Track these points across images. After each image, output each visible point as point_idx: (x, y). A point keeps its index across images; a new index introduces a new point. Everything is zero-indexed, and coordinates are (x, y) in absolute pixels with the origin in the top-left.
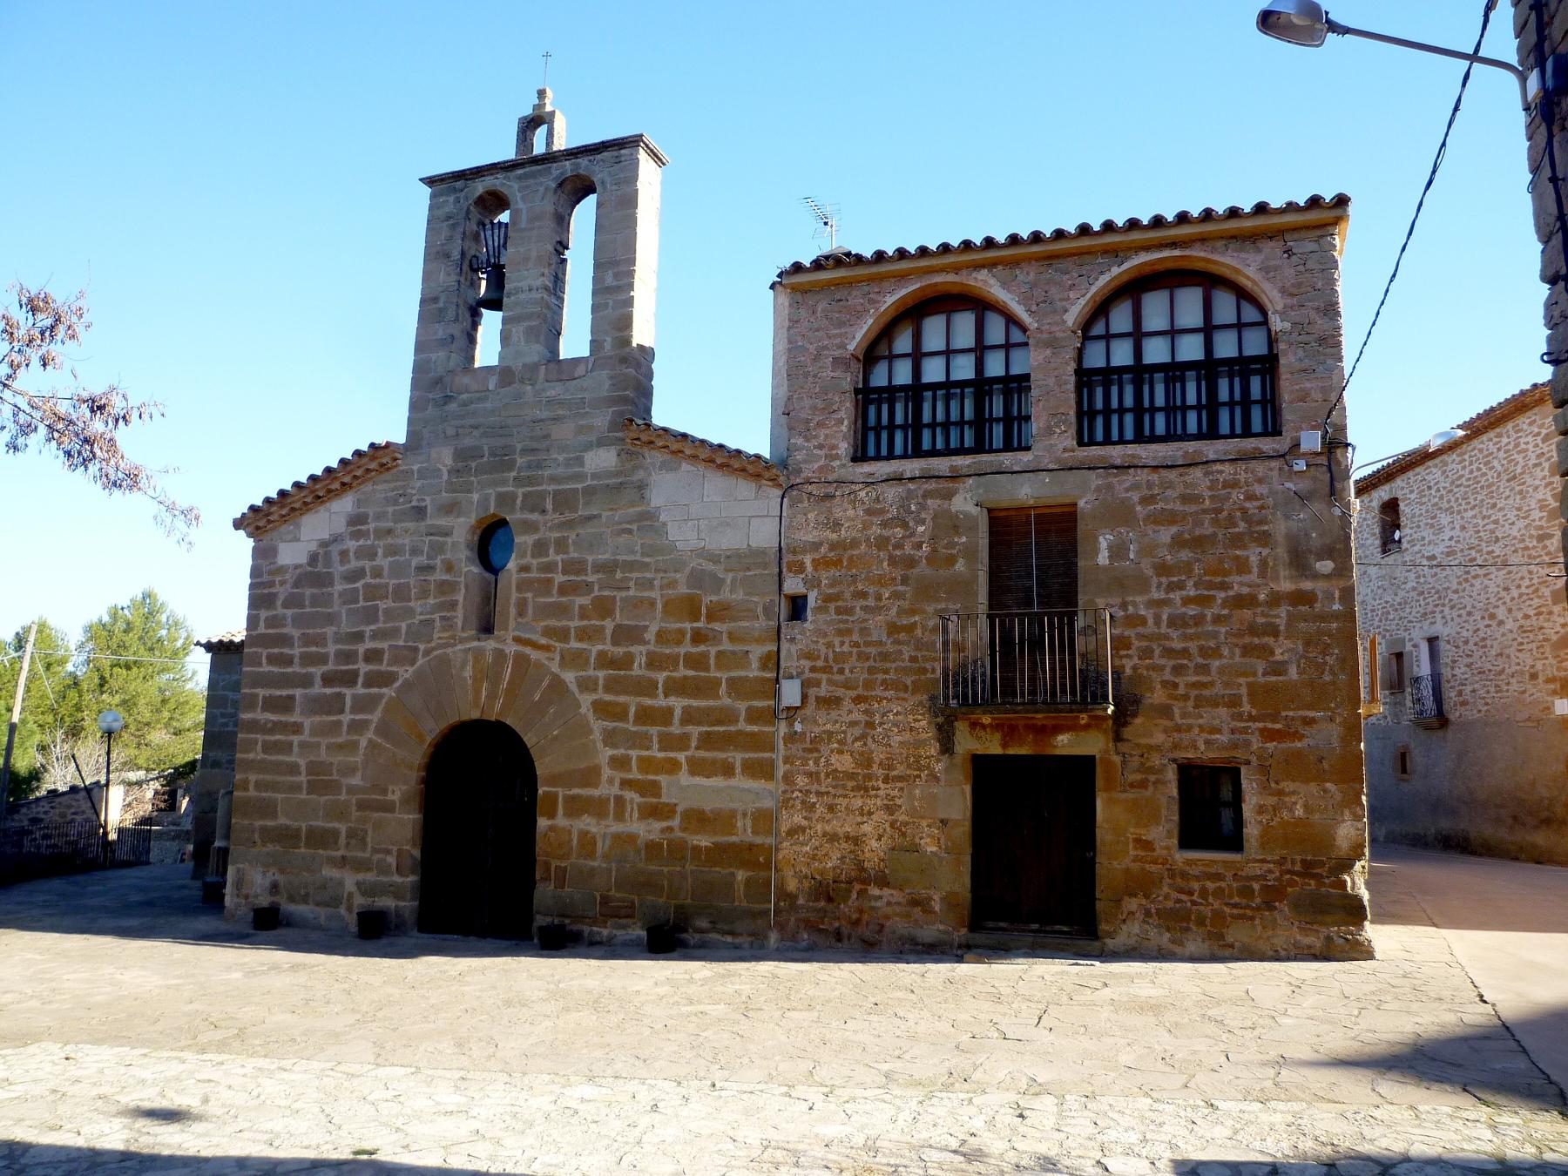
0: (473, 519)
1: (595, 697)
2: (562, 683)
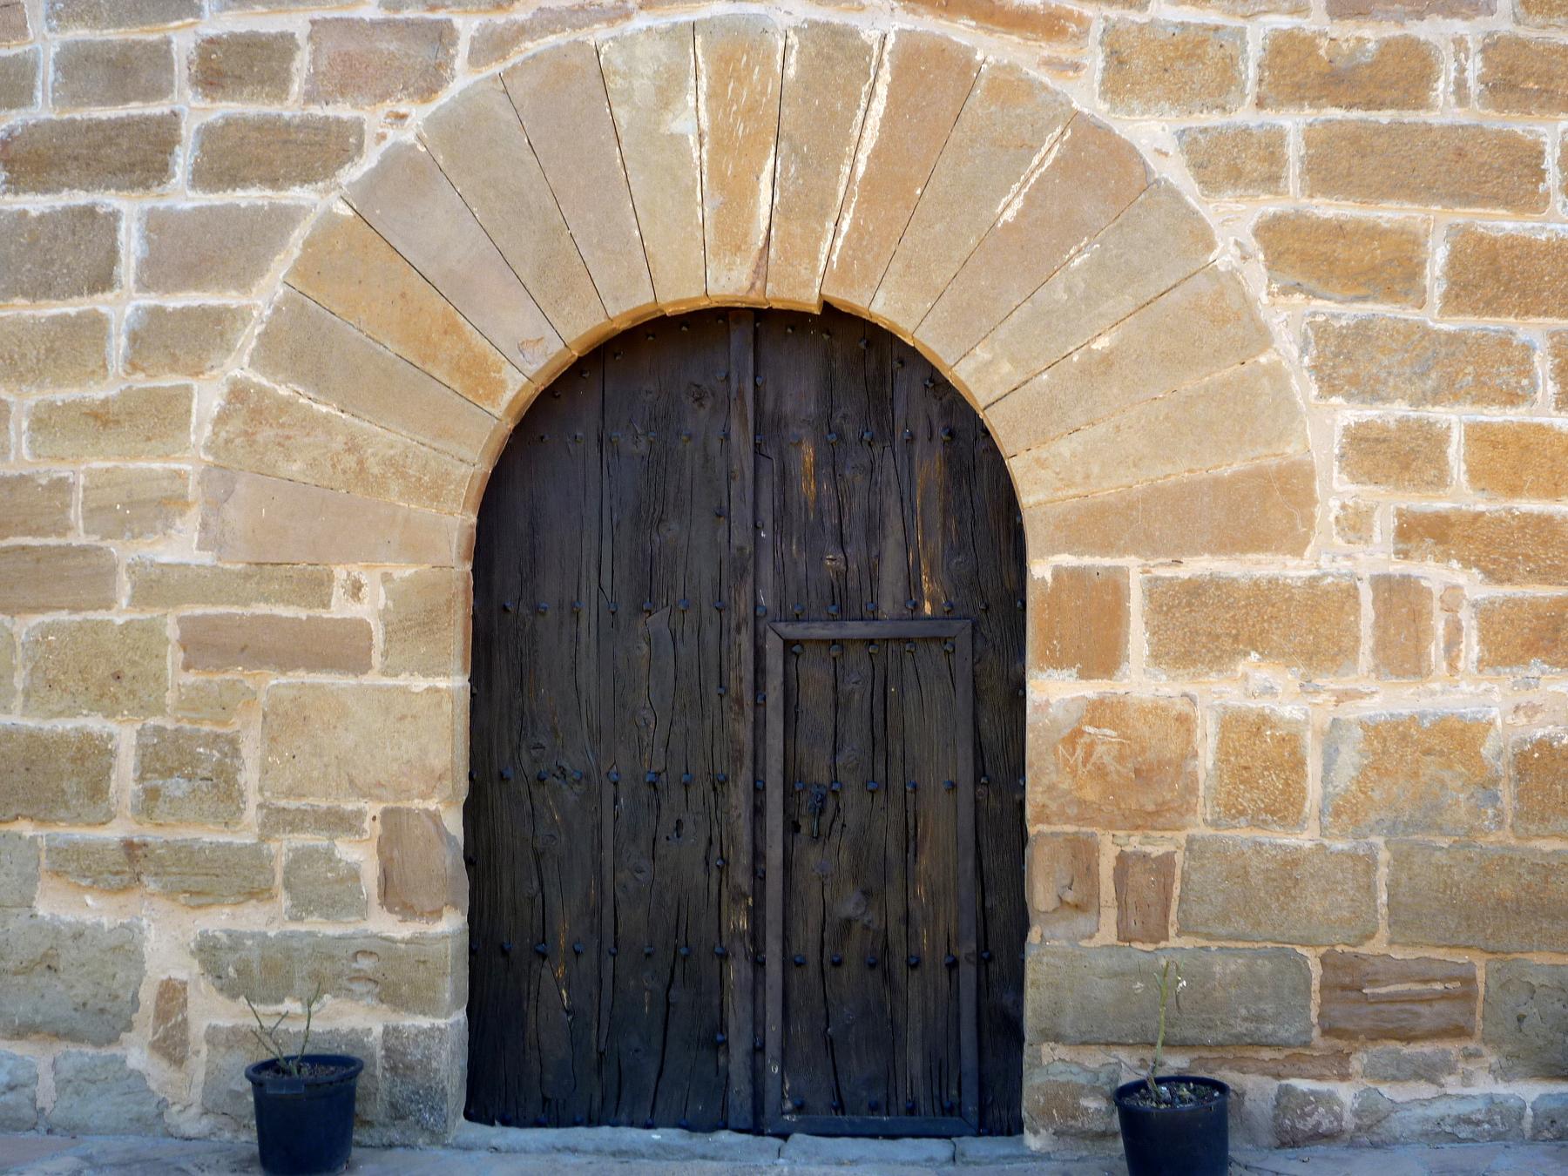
1: (1270, 206)
2: (1123, 154)
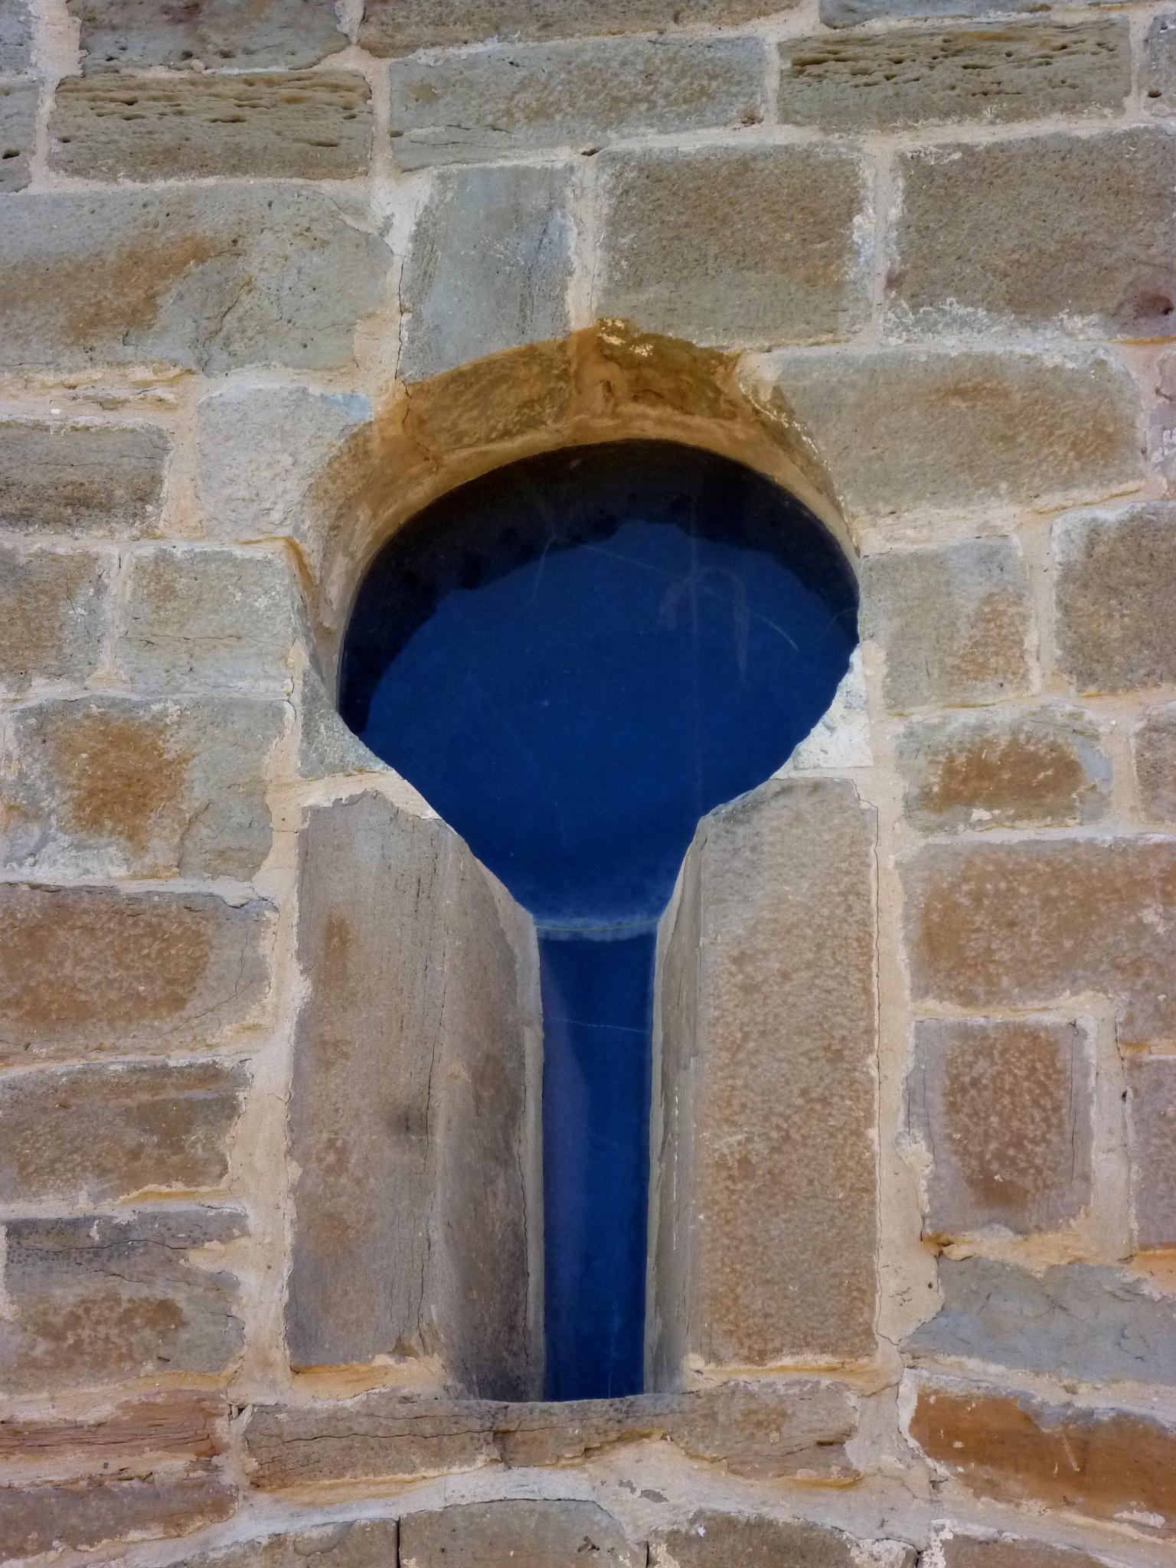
0: (372, 387)
